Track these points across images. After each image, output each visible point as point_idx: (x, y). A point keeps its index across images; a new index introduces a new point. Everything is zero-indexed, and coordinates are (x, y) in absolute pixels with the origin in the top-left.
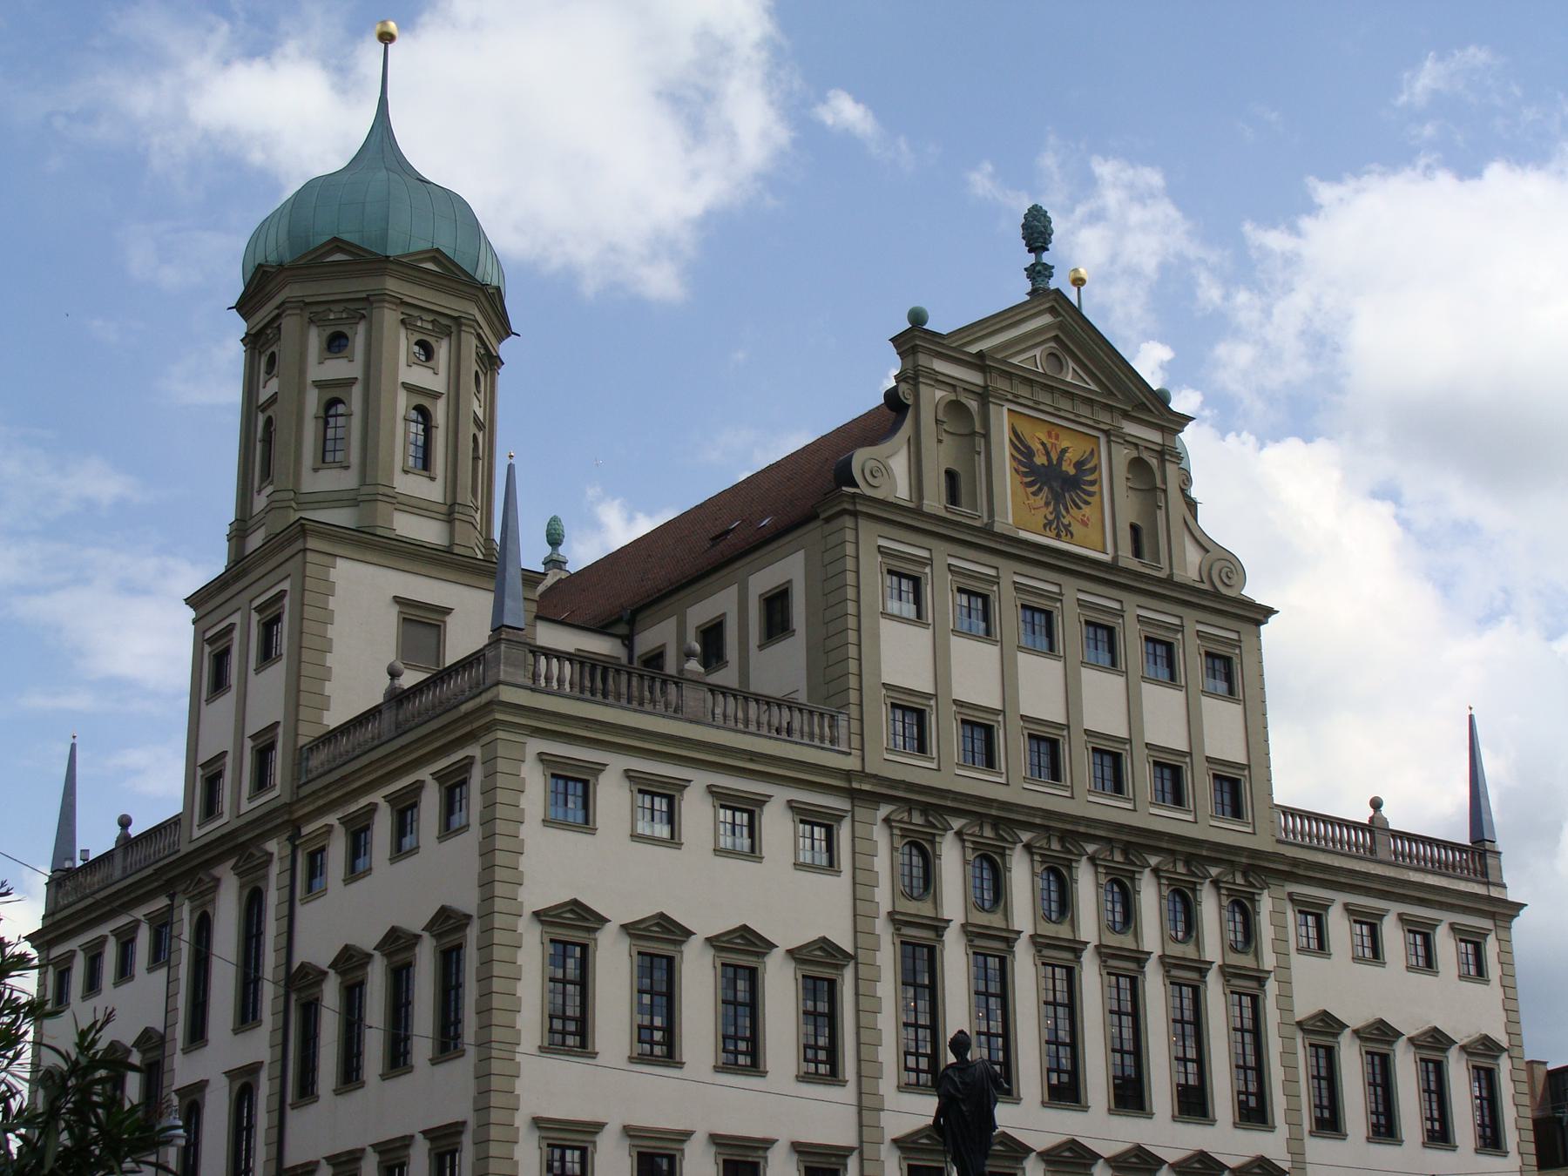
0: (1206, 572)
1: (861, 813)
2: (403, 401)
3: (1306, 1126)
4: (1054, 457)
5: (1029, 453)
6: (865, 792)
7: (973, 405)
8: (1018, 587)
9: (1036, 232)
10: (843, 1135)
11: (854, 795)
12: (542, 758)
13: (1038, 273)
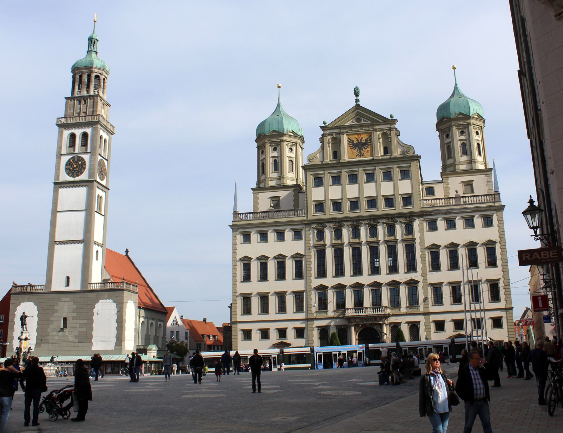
0: (403, 153)
3: (428, 270)
4: (359, 140)
5: (353, 141)
6: (308, 223)
10: (302, 288)
11: (305, 224)
13: (357, 100)
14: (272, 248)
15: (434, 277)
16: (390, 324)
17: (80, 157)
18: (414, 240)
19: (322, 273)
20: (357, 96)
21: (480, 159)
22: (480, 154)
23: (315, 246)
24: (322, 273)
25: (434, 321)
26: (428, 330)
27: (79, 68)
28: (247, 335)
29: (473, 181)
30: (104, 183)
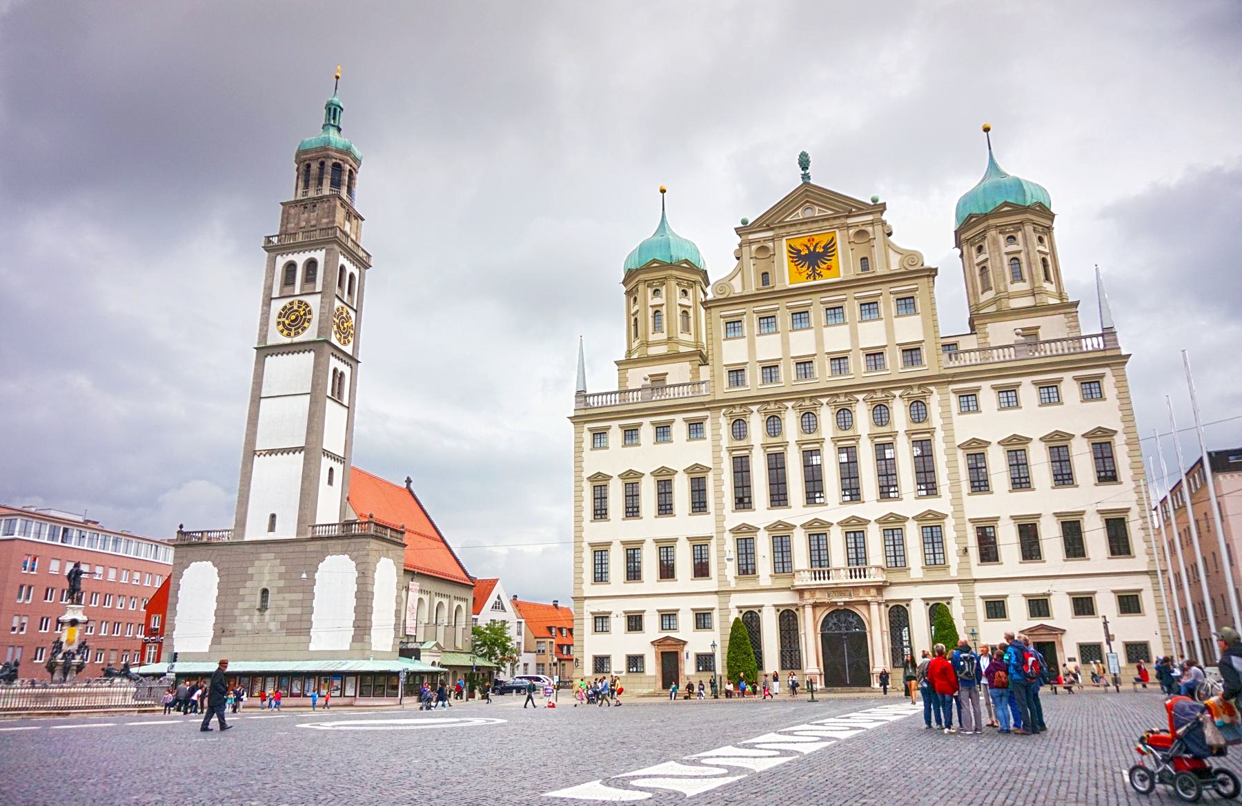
1: (715, 414)
2: (651, 312)
7: (770, 245)
8: (788, 308)
9: (804, 162)
11: (708, 409)
12: (590, 430)
13: (806, 177)
14: (647, 456)
15: (979, 507)
16: (887, 603)
17: (300, 302)
18: (931, 431)
19: (743, 501)
20: (805, 168)
21: (1050, 287)
22: (1047, 278)
23: (731, 450)
24: (743, 501)
25: (983, 597)
26: (970, 616)
27: (306, 152)
28: (601, 620)
29: (1038, 328)
30: (348, 349)
